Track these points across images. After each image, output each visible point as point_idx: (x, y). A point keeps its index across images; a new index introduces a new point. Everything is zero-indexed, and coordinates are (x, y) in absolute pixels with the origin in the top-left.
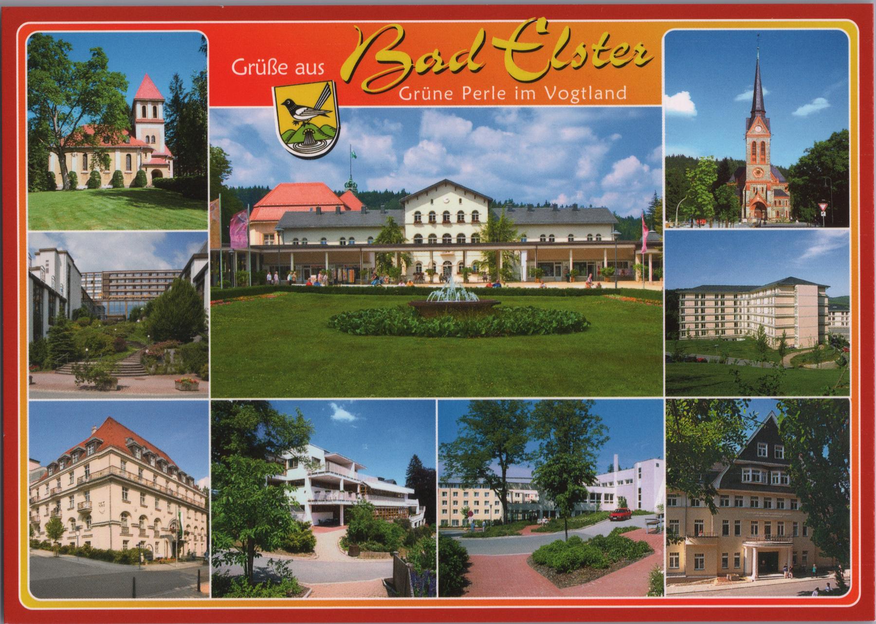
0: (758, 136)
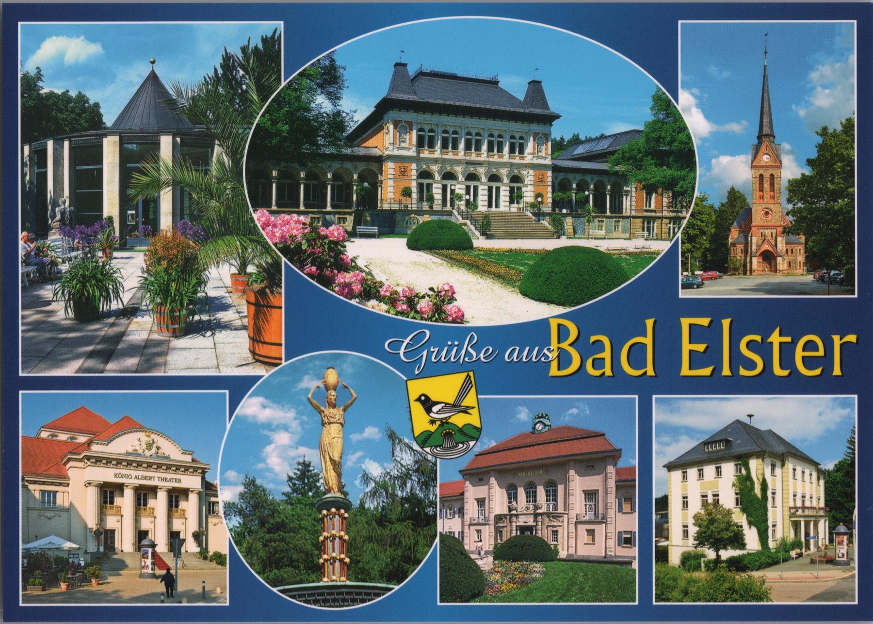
0: (766, 167)
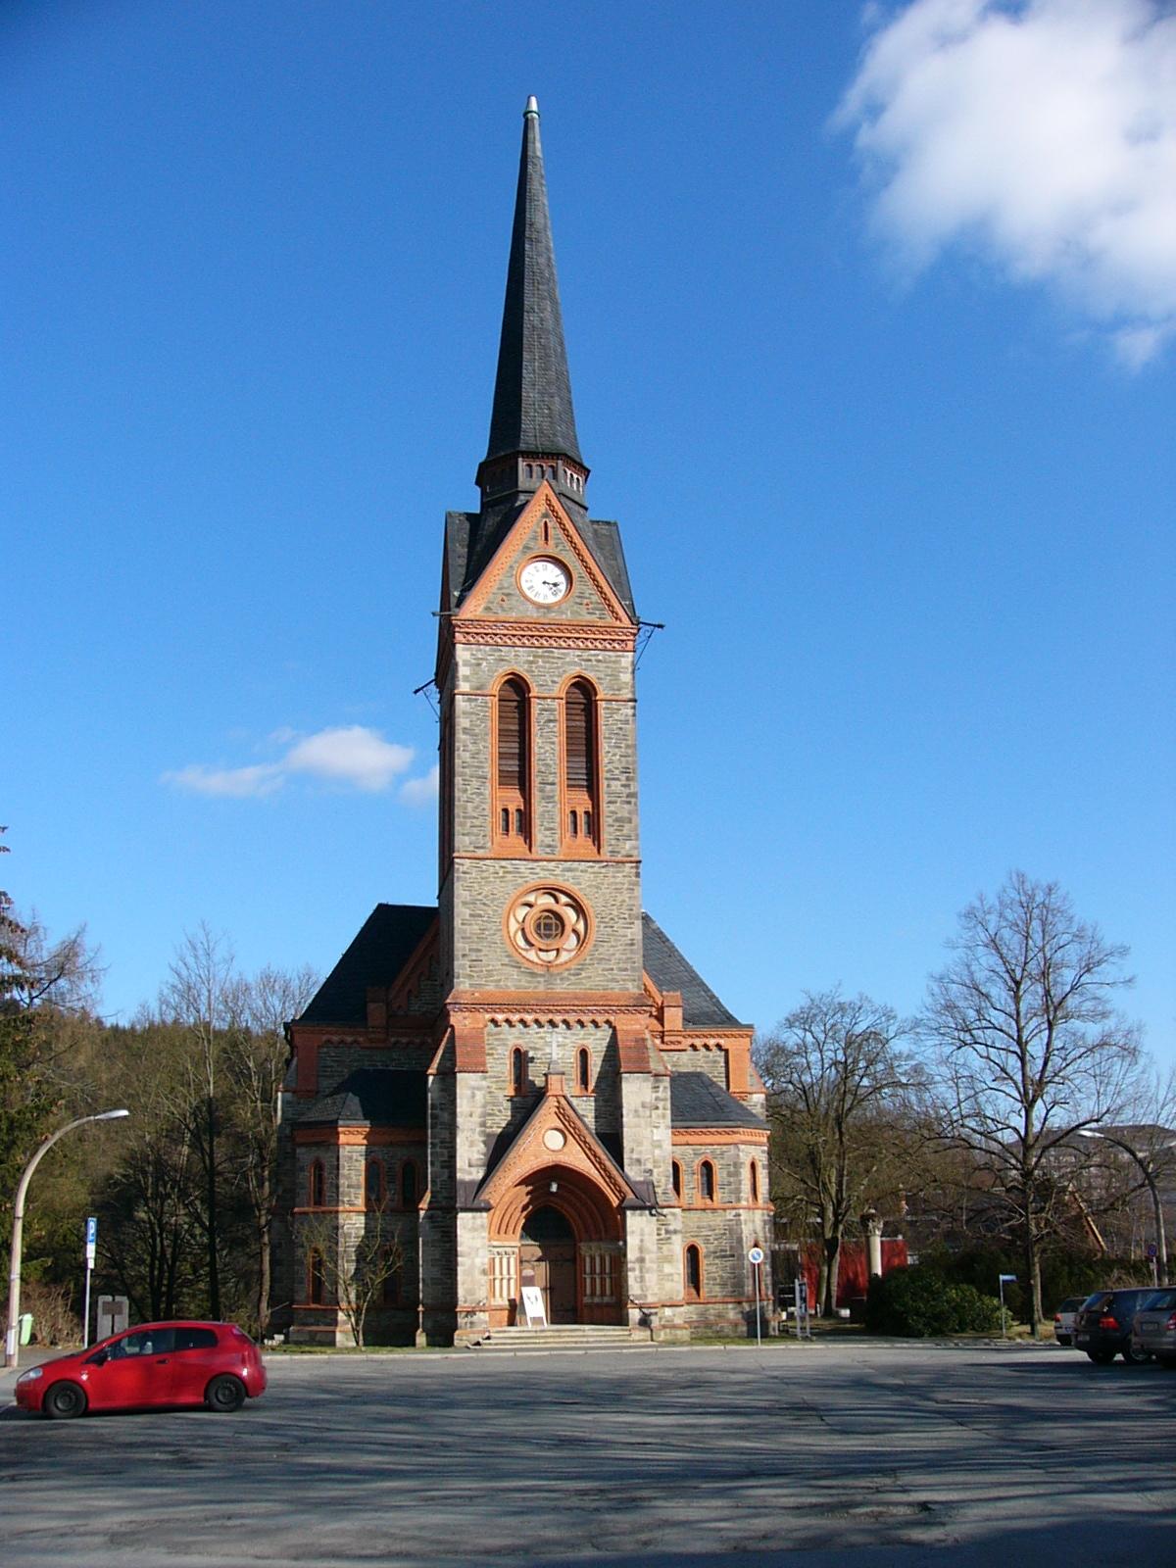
0: (541, 631)
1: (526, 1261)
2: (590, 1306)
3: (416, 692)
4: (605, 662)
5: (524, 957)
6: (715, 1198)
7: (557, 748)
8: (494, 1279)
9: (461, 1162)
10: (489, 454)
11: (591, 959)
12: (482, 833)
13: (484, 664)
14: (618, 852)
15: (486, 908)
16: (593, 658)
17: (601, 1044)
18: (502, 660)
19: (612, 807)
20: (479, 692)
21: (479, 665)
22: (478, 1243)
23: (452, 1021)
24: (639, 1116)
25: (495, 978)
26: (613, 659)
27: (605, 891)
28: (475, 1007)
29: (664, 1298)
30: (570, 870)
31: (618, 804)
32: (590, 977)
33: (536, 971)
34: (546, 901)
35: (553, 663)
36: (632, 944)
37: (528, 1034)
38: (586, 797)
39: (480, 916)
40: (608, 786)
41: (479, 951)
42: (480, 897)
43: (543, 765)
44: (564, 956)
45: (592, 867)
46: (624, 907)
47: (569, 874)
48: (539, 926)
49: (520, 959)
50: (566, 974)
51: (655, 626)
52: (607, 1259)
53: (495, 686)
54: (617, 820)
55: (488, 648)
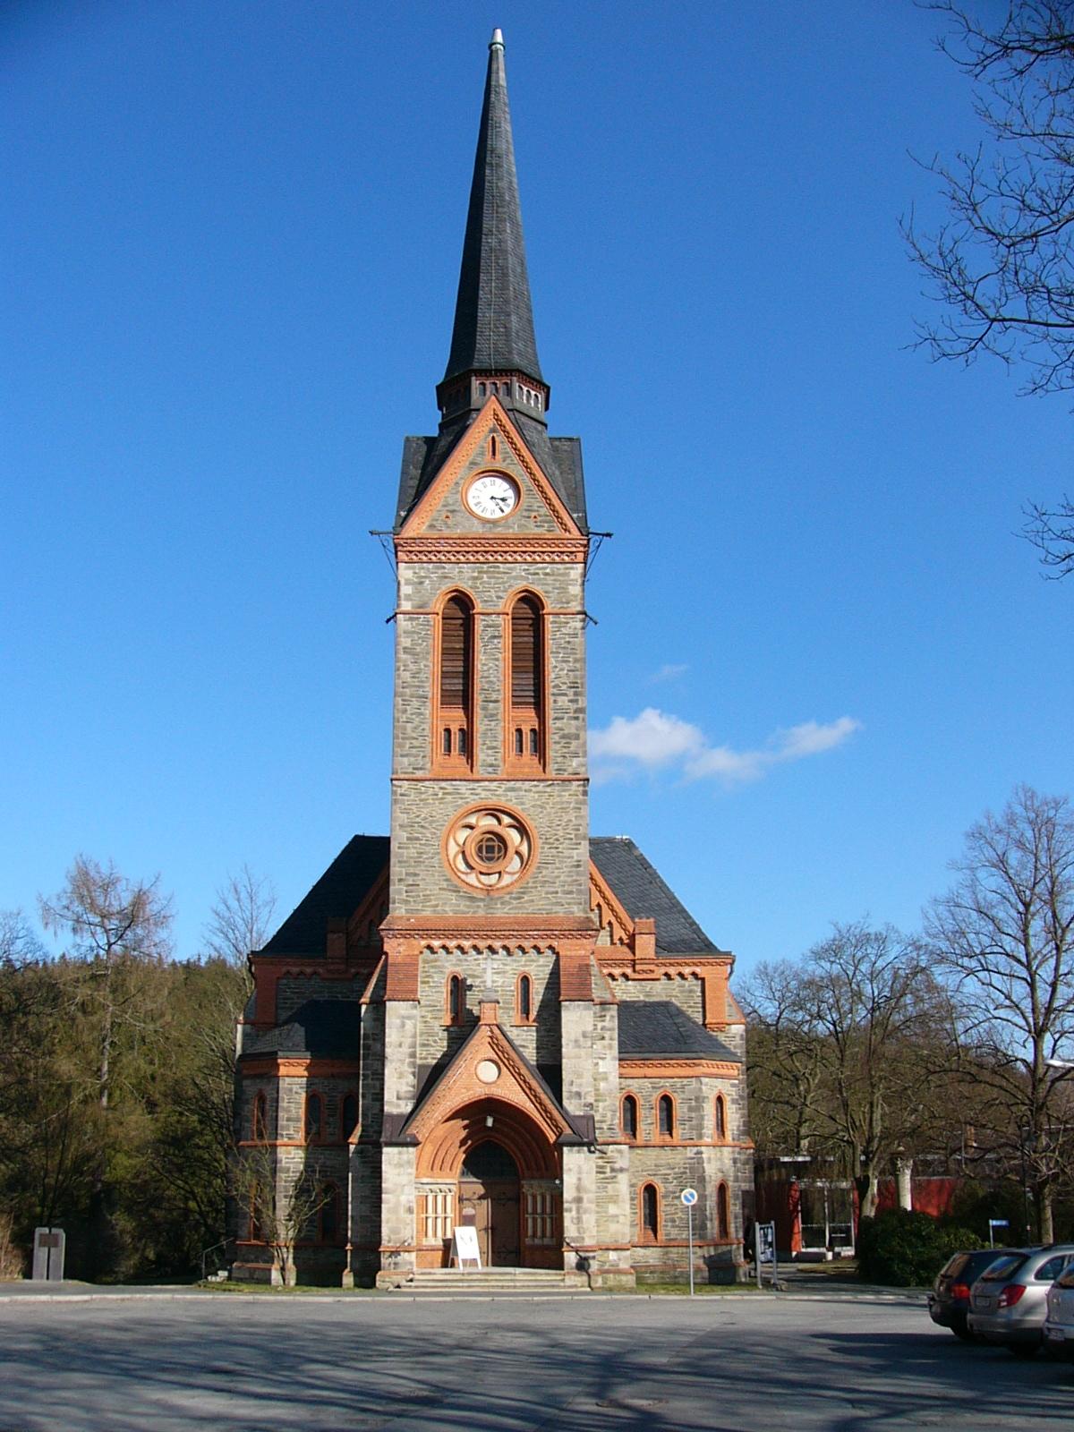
1: (467, 1199)
2: (534, 1248)
3: (388, 621)
4: (553, 575)
5: (463, 881)
6: (674, 1135)
7: (501, 664)
8: (427, 1218)
9: (389, 1095)
10: (446, 376)
11: (534, 882)
12: (422, 754)
13: (427, 582)
14: (565, 770)
15: (424, 831)
16: (540, 572)
17: (543, 971)
18: (446, 577)
19: (559, 724)
20: (421, 610)
21: (421, 583)
22: (404, 1179)
23: (386, 948)
24: (579, 1047)
25: (433, 903)
26: (561, 571)
27: (549, 810)
28: (408, 933)
29: (607, 1239)
30: (513, 790)
31: (565, 721)
32: (532, 901)
33: (475, 895)
34: (489, 822)
35: (498, 578)
36: (578, 866)
37: (466, 960)
38: (533, 714)
39: (417, 839)
40: (555, 701)
41: (416, 875)
42: (418, 820)
43: (487, 682)
44: (507, 879)
45: (536, 786)
46: (571, 827)
47: (513, 794)
48: (480, 849)
49: (457, 882)
50: (507, 898)
51: (603, 535)
52: (548, 1198)
53: (439, 605)
54: (563, 737)
55: (431, 566)
